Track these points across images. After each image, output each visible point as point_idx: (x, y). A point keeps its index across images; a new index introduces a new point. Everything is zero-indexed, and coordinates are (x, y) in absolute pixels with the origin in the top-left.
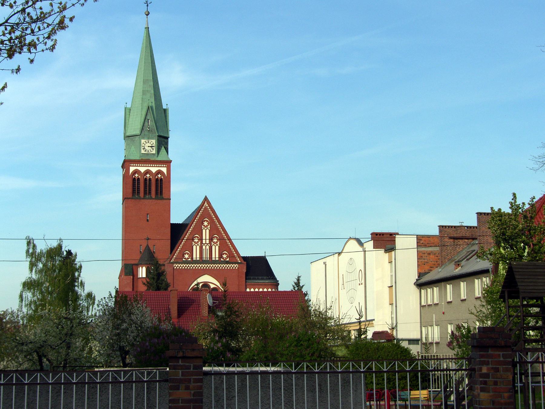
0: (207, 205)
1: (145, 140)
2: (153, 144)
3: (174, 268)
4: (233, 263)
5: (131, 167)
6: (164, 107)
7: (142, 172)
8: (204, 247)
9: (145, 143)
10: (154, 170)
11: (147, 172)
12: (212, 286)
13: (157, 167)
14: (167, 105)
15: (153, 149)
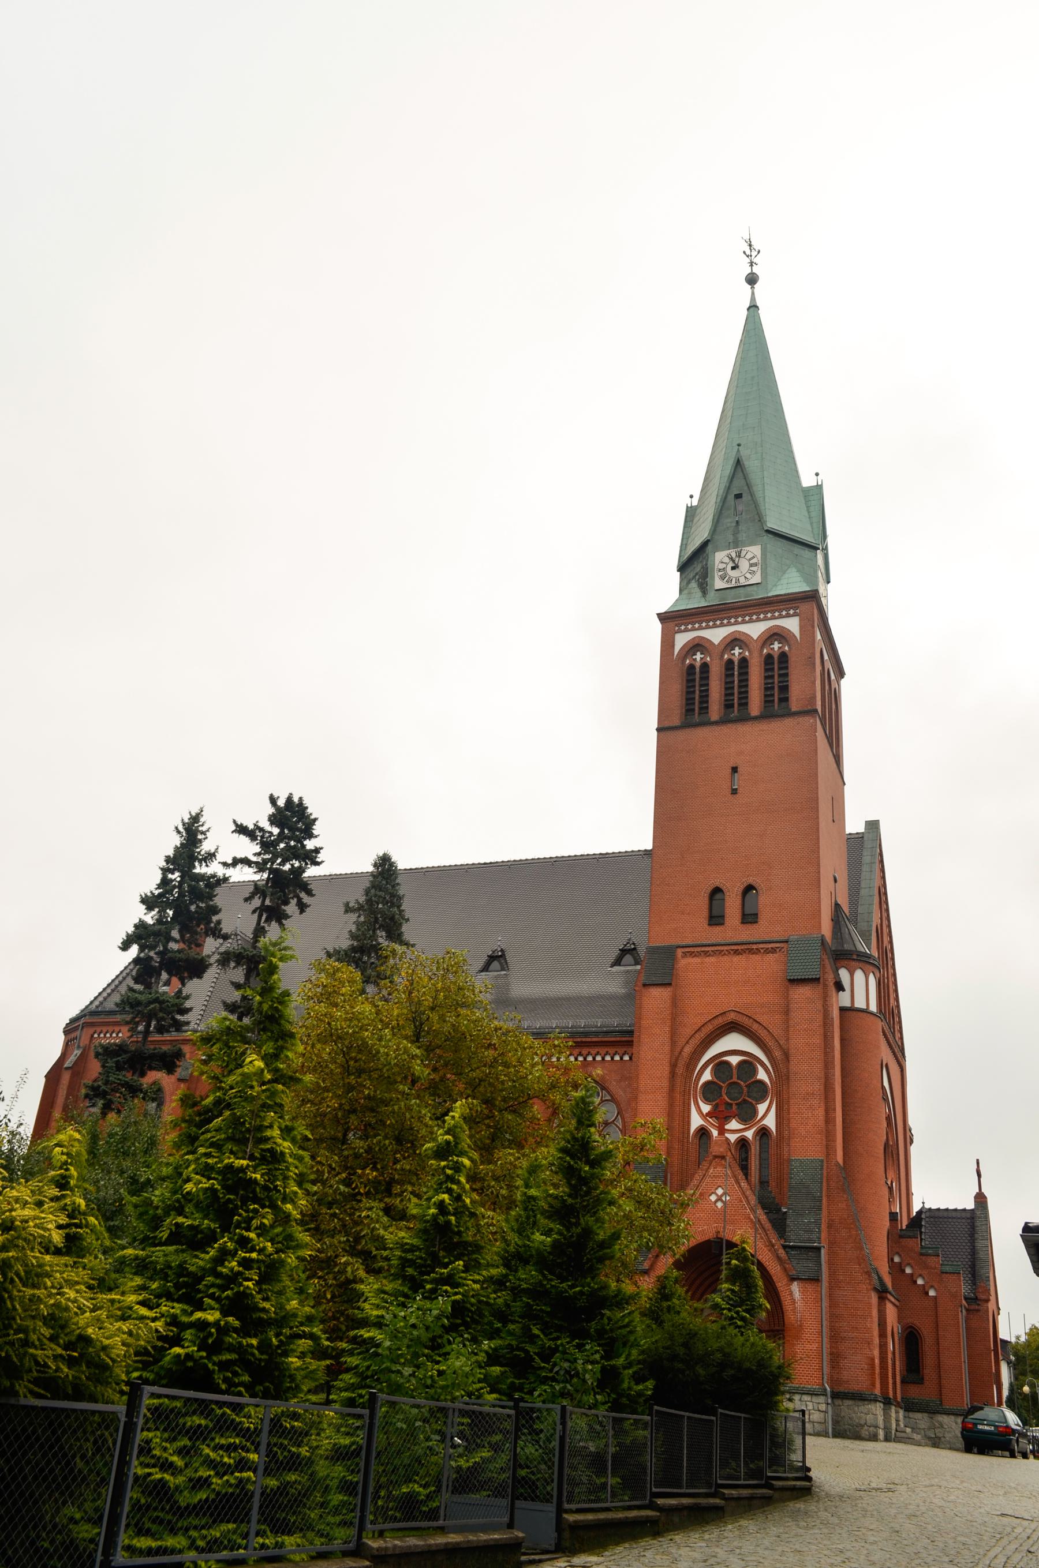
1: (728, 552)
2: (753, 557)
6: (807, 480)
7: (716, 643)
9: (727, 560)
10: (755, 630)
14: (817, 474)
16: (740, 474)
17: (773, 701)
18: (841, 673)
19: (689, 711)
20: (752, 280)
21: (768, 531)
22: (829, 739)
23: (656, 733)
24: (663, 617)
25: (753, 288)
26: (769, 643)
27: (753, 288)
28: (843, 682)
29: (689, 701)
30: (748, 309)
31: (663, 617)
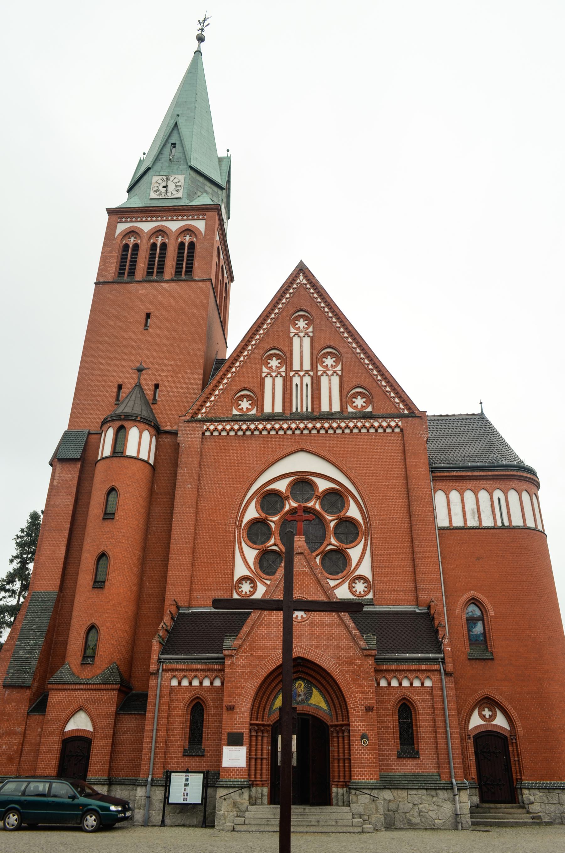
0: (304, 281)
1: (162, 177)
2: (179, 182)
3: (203, 434)
4: (384, 417)
8: (296, 380)
9: (160, 181)
10: (174, 226)
11: (160, 231)
12: (323, 485)
15: (177, 191)
16: (175, 132)
17: (181, 272)
18: (232, 279)
19: (121, 274)
21: (192, 168)
22: (218, 308)
23: (94, 285)
24: (111, 212)
26: (183, 235)
28: (232, 284)
29: (122, 267)
30: (195, 53)
31: (111, 212)
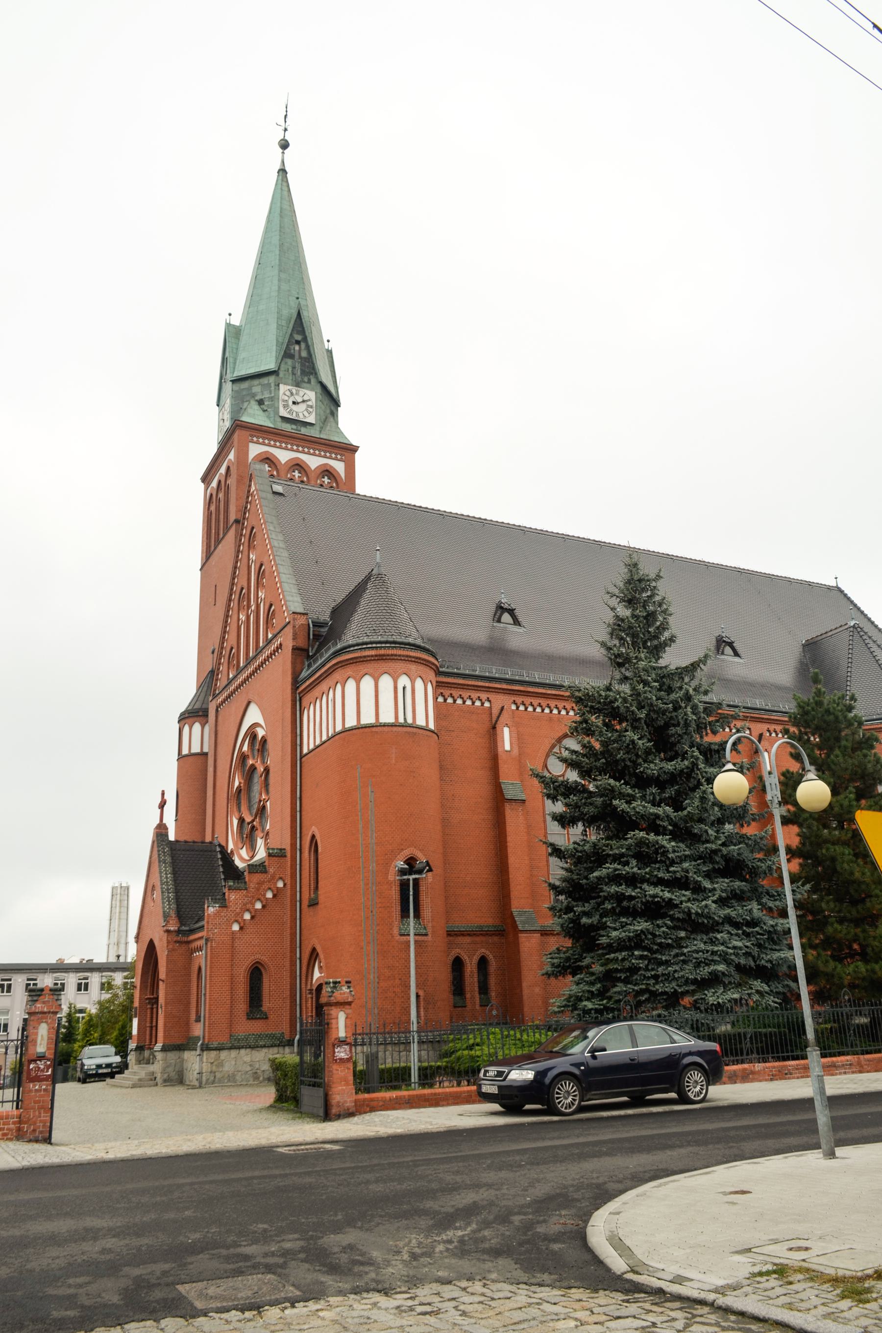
2: (309, 400)
5: (251, 445)
7: (283, 462)
9: (288, 393)
13: (320, 456)
15: (310, 413)
20: (284, 145)
25: (283, 153)
27: (283, 153)
